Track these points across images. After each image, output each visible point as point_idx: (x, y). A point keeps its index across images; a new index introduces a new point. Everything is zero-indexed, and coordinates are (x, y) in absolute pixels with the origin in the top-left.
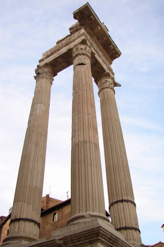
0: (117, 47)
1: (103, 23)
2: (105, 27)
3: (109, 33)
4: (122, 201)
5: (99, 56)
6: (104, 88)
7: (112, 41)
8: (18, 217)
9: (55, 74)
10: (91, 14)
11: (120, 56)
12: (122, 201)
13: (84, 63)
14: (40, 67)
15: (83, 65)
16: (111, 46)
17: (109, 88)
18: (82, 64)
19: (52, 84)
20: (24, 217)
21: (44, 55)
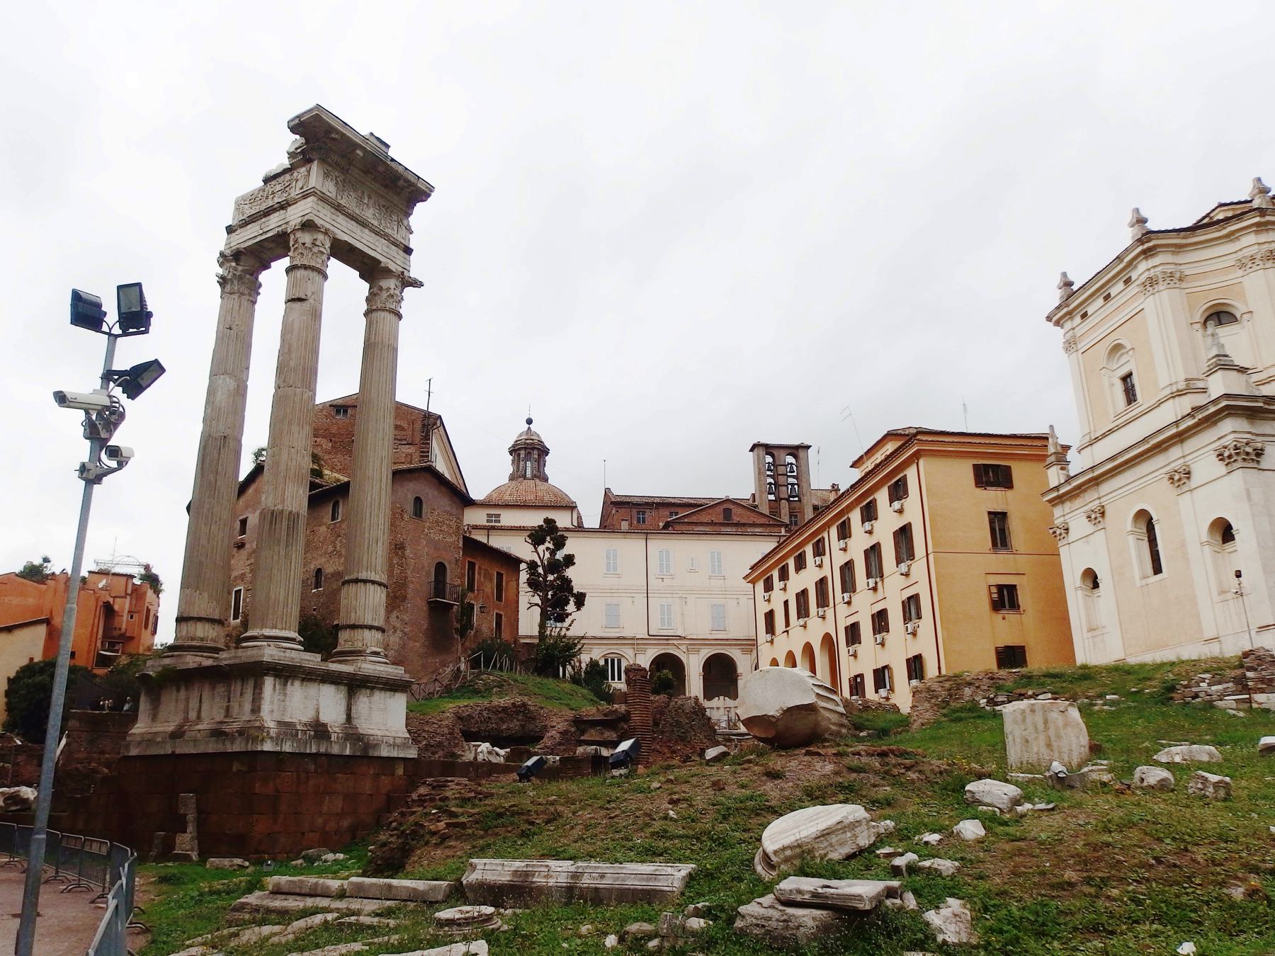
0: (419, 177)
1: (372, 134)
2: (379, 145)
3: (392, 153)
4: (357, 581)
5: (363, 224)
6: (374, 310)
7: (400, 169)
8: (185, 615)
9: (267, 267)
10: (331, 129)
11: (429, 196)
12: (357, 581)
13: (304, 297)
14: (226, 256)
15: (299, 303)
16: (401, 183)
17: (383, 310)
18: (300, 300)
19: (254, 303)
20: (196, 616)
21: (239, 205)
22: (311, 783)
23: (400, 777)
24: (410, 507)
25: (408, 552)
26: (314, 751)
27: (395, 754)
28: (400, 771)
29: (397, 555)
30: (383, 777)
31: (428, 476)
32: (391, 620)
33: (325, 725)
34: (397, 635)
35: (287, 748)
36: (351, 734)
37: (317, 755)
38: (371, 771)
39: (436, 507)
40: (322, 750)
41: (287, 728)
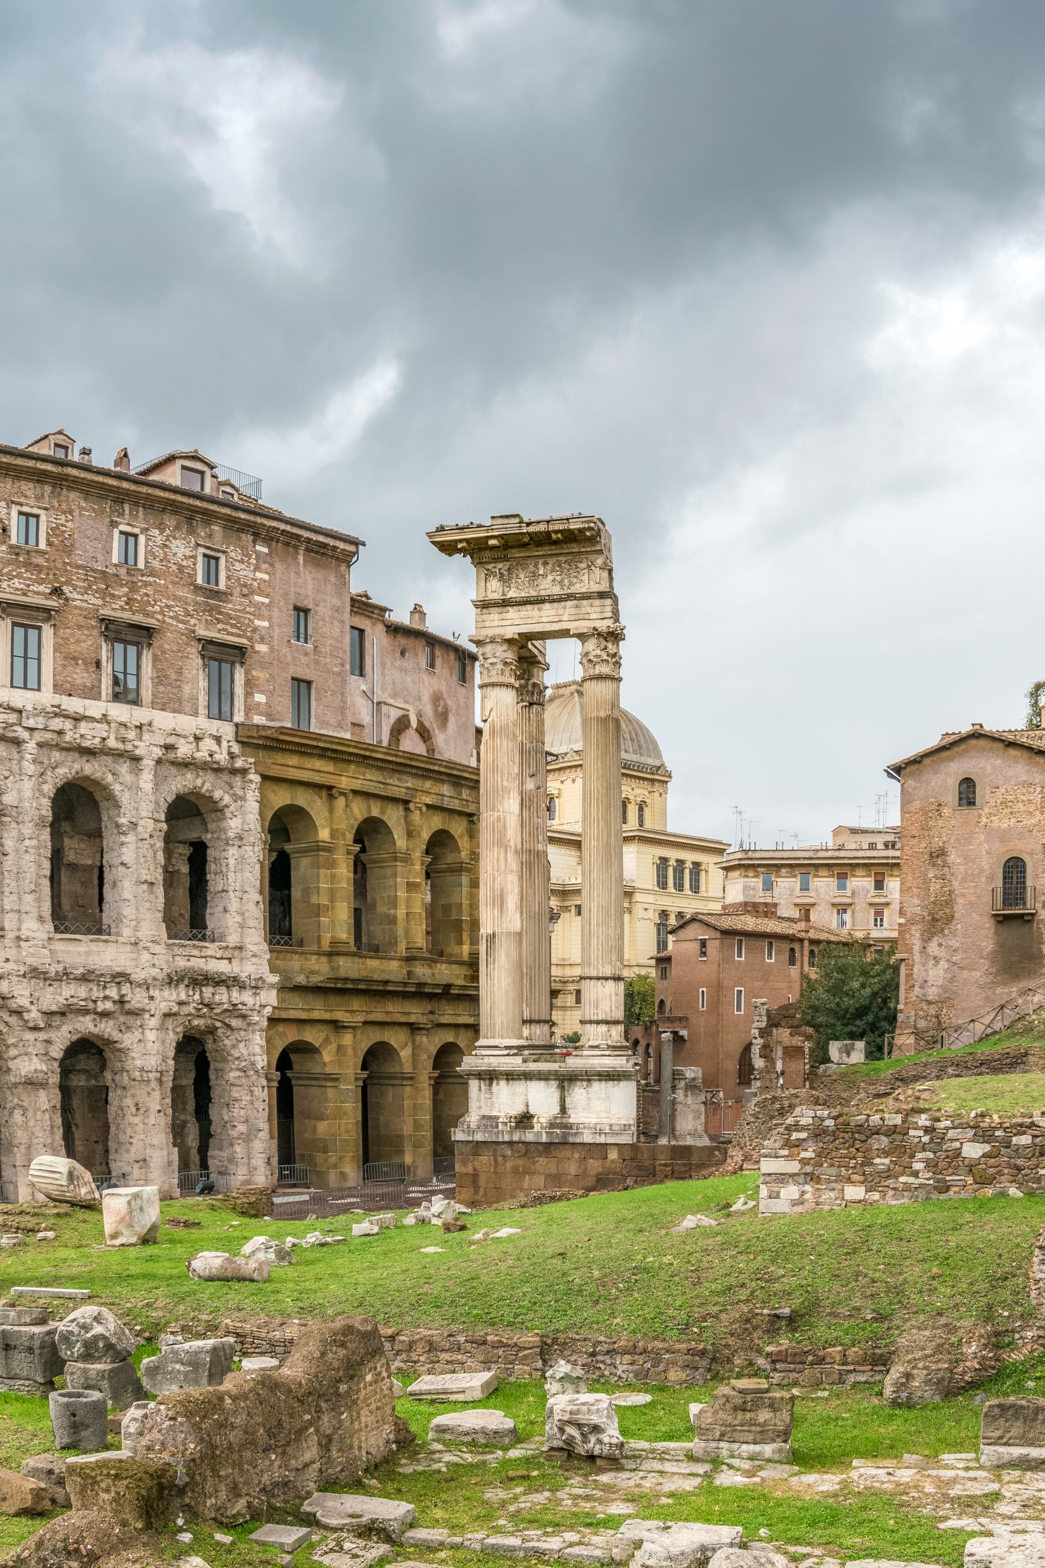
22: (509, 1165)
23: (613, 1161)
24: (951, 797)
25: (953, 858)
26: (507, 1138)
27: (602, 1140)
28: (613, 1155)
29: (934, 866)
30: (591, 1161)
31: (982, 742)
32: (929, 950)
33: (532, 1116)
34: (940, 966)
35: (479, 1137)
36: (561, 1122)
37: (511, 1143)
38: (577, 1155)
39: (1000, 783)
40: (516, 1137)
41: (489, 1121)
